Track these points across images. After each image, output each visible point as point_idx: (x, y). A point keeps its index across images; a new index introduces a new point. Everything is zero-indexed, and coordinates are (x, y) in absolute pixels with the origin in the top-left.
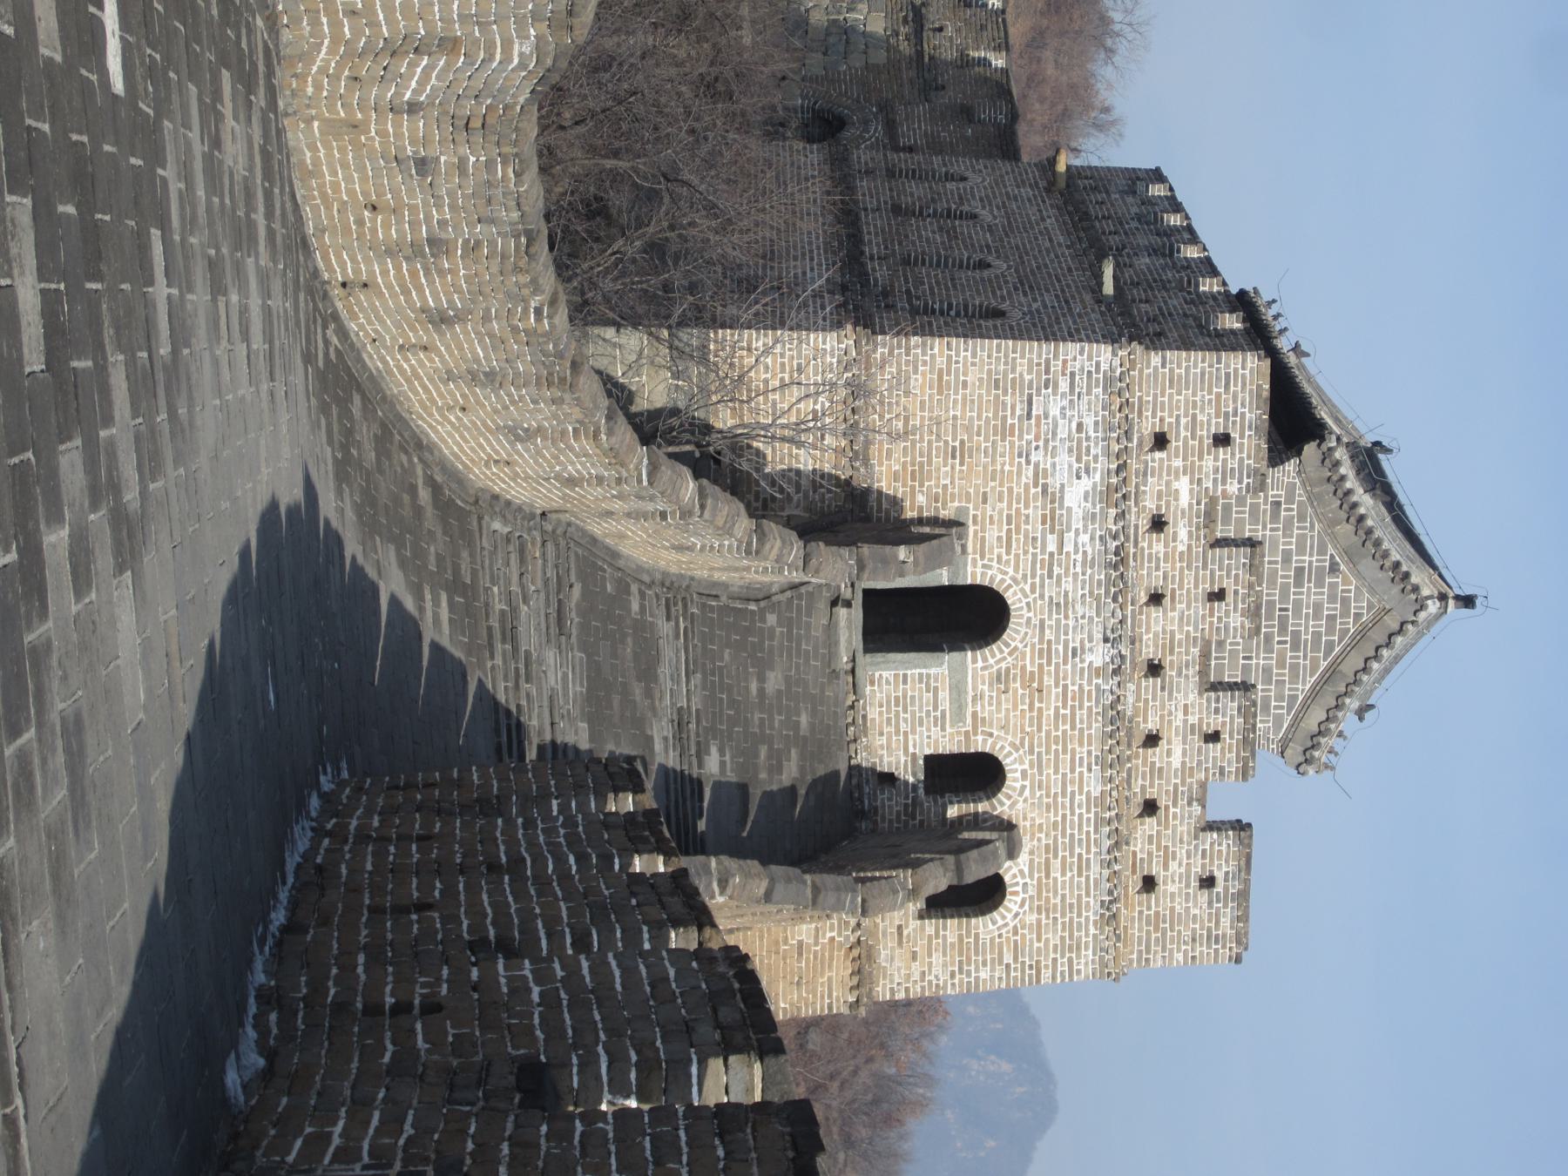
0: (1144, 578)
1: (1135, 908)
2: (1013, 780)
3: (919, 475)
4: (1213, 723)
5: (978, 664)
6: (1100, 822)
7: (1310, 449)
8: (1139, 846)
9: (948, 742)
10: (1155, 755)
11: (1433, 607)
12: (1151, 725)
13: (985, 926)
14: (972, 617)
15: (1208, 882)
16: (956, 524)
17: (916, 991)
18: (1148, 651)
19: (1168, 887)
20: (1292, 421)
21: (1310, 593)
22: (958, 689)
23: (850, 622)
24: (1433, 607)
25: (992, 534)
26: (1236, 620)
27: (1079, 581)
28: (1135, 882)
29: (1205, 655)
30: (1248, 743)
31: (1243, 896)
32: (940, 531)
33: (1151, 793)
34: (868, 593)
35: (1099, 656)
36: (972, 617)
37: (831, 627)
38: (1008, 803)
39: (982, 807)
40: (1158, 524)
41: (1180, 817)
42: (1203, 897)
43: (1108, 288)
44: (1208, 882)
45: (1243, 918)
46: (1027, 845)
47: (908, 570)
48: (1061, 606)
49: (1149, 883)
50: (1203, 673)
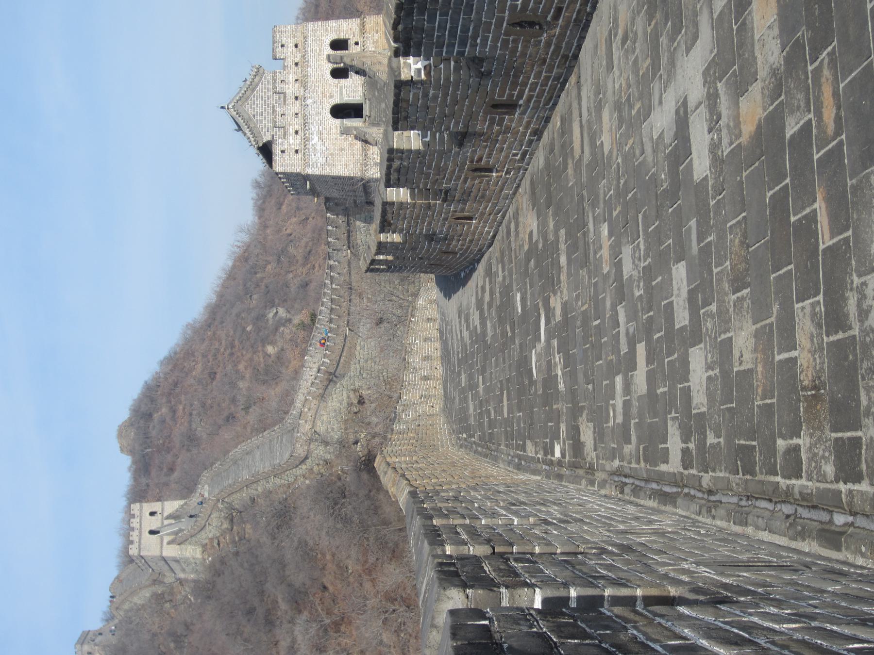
0: (300, 120)
1: (299, 40)
2: (328, 72)
3: (351, 145)
4: (282, 85)
5: (337, 100)
6: (308, 61)
7: (261, 145)
8: (299, 55)
9: (343, 82)
10: (296, 77)
11: (230, 106)
12: (297, 85)
13: (334, 36)
15: (282, 46)
16: (342, 133)
17: (350, 20)
18: (298, 102)
19: (292, 45)
20: (266, 151)
21: (259, 110)
22: (341, 94)
23: (366, 111)
24: (230, 106)
25: (334, 131)
26: (278, 109)
27: (314, 120)
28: (299, 46)
29: (285, 101)
30: (274, 80)
31: (274, 42)
32: (345, 131)
33: (296, 68)
34: (361, 116)
35: (309, 101)
37: (370, 111)
38: (329, 67)
39: (335, 66)
40: (297, 132)
41: (289, 62)
42: (283, 42)
43: (308, 183)
44: (282, 46)
45: (274, 37)
46: (325, 57)
48: (318, 114)
49: (296, 46)
50: (285, 97)
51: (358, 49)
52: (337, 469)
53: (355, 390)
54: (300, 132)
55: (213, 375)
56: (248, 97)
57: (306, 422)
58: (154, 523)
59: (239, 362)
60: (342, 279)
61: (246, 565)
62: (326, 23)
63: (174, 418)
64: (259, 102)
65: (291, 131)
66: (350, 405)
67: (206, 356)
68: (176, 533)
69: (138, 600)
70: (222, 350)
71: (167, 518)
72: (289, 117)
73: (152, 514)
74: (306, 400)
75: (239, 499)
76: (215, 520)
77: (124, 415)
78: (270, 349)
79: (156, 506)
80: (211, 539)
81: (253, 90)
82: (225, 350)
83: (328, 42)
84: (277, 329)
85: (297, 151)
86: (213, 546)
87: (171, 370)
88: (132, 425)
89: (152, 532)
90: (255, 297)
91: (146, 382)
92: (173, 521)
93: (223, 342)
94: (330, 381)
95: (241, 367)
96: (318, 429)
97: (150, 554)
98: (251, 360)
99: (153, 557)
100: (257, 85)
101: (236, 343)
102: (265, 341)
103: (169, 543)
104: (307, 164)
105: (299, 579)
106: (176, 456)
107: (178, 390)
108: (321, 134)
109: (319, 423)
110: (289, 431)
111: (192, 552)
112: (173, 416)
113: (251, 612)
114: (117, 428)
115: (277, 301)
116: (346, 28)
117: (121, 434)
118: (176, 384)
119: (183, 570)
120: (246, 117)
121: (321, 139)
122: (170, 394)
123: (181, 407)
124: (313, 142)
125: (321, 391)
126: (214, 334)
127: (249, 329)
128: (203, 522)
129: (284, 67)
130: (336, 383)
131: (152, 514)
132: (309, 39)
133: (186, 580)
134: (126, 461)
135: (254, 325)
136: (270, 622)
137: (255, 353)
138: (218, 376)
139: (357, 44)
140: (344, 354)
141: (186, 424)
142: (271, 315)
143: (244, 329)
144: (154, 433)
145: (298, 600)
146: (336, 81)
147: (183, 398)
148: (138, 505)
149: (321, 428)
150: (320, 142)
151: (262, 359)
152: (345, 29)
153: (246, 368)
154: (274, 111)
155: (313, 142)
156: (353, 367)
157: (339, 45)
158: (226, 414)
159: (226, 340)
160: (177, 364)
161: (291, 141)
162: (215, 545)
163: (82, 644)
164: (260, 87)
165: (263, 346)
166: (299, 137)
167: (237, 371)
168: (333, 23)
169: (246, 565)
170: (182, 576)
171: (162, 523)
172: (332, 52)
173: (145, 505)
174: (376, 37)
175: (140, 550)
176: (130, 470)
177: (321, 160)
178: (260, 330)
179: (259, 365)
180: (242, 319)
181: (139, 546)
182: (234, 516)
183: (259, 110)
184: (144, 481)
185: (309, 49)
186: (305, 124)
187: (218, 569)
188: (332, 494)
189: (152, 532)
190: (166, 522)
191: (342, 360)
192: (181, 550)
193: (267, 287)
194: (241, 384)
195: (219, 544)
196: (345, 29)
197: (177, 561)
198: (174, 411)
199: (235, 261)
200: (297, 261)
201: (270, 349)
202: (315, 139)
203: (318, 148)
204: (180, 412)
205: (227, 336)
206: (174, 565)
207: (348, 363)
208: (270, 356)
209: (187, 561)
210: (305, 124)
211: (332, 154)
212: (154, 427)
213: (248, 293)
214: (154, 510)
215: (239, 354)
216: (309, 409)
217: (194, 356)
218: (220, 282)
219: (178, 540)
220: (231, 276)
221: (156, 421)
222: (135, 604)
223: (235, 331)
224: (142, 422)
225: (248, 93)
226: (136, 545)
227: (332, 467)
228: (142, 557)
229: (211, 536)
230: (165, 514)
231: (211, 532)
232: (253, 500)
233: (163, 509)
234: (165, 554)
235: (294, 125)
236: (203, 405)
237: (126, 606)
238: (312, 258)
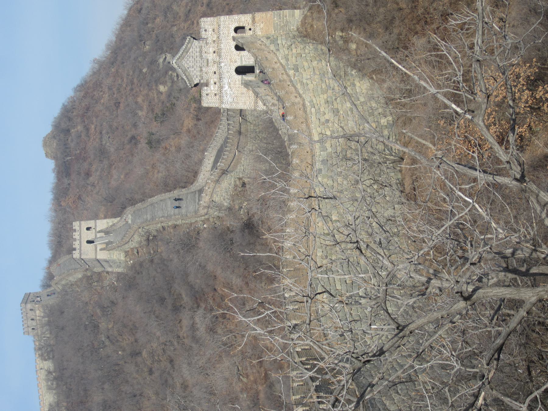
1: (216, 27)
5: (239, 64)
8: (216, 36)
10: (214, 50)
15: (205, 30)
17: (246, 15)
25: (238, 82)
27: (226, 75)
29: (208, 64)
35: (222, 65)
38: (233, 44)
41: (210, 41)
47: (249, 77)
48: (228, 72)
51: (251, 33)
52: (228, 223)
53: (240, 179)
54: (217, 83)
55: (117, 104)
56: (184, 57)
57: (206, 195)
58: (90, 236)
59: (137, 96)
60: (235, 129)
61: (159, 270)
62: (231, 17)
63: (88, 136)
64: (191, 59)
65: (212, 82)
66: (236, 186)
67: (112, 89)
68: (107, 244)
69: (72, 279)
70: (124, 86)
71: (100, 232)
72: (211, 74)
73: (88, 229)
74: (207, 183)
75: (153, 228)
76: (137, 238)
77: (48, 129)
78: (162, 88)
79: (91, 223)
80: (132, 249)
81: (187, 52)
82: (126, 86)
83: (233, 28)
84: (166, 73)
85: (215, 95)
86: (134, 254)
87: (84, 97)
88: (54, 137)
89: (89, 242)
90: (148, 43)
91: (63, 105)
92: (102, 234)
93: (125, 80)
94: (223, 173)
95: (140, 100)
96: (214, 199)
97: (88, 257)
98: (147, 95)
99: (91, 260)
100: (189, 49)
101: (135, 81)
102: (158, 82)
103: (101, 250)
104: (222, 102)
105: (197, 281)
106: (91, 164)
107: (90, 114)
108: (230, 84)
109: (215, 196)
110: (192, 192)
111: (118, 256)
112: (87, 133)
113: (162, 300)
114: (43, 139)
115: (165, 49)
116: (244, 20)
117: (46, 143)
118: (88, 109)
119: (111, 266)
120: (184, 69)
121: (230, 87)
122: (83, 116)
123: (93, 127)
124: (225, 89)
125: (217, 178)
126: (117, 71)
127: (144, 70)
128: (128, 240)
129: (207, 43)
130: (227, 174)
131: (88, 229)
132: (222, 26)
133: (112, 272)
134: (50, 164)
135: (148, 67)
136: (177, 309)
137: (150, 90)
138: (121, 105)
139: (250, 29)
140: (234, 161)
141: (97, 140)
142: (161, 60)
143: (141, 71)
144: (72, 145)
145: (198, 297)
146: (238, 52)
147: (94, 119)
148: (78, 222)
149: (216, 198)
150: (229, 89)
151: (155, 95)
152: (243, 20)
153: (143, 101)
154: (201, 70)
155: (225, 89)
156: (239, 168)
158: (130, 136)
159: (127, 79)
160: (88, 90)
161: (212, 88)
162: (135, 252)
163: (26, 303)
164: (191, 50)
165: (157, 85)
166: (216, 86)
167: (136, 103)
168: (236, 17)
169: (159, 270)
170: (110, 269)
171: (96, 235)
172: (235, 35)
173: (83, 222)
174: (262, 26)
175: (81, 255)
176: (54, 172)
177: (230, 100)
178: (153, 73)
179: (154, 99)
180: (140, 62)
181: (80, 252)
182: (150, 239)
183: (191, 64)
184: (66, 181)
185: (221, 33)
186: (220, 79)
187: (138, 269)
188: (223, 238)
189: (89, 242)
190: (99, 235)
191: (232, 164)
192: (110, 254)
193: (157, 37)
194: (140, 113)
195: (138, 253)
196: (243, 20)
197: (106, 261)
198: (88, 130)
199: (130, 10)
200: (180, 18)
201: (162, 88)
202: (226, 87)
203: (228, 92)
204: (92, 130)
205: (128, 75)
206: (104, 263)
207: (236, 166)
208: (162, 93)
209: (114, 262)
210: (220, 79)
211: (236, 96)
212: (72, 141)
213: (141, 39)
214: (89, 226)
215: (138, 90)
216: (209, 188)
217: (102, 87)
218: (118, 27)
219: (108, 247)
220: (126, 23)
221: (73, 135)
222: (70, 281)
223: (134, 72)
224: (62, 135)
225: (184, 54)
226: (78, 251)
227: (223, 221)
228: (82, 259)
229: (132, 247)
230: (98, 229)
231: (133, 244)
232: (164, 228)
233: (96, 226)
234: (98, 257)
236: (111, 127)
237: (63, 282)
238: (191, 16)
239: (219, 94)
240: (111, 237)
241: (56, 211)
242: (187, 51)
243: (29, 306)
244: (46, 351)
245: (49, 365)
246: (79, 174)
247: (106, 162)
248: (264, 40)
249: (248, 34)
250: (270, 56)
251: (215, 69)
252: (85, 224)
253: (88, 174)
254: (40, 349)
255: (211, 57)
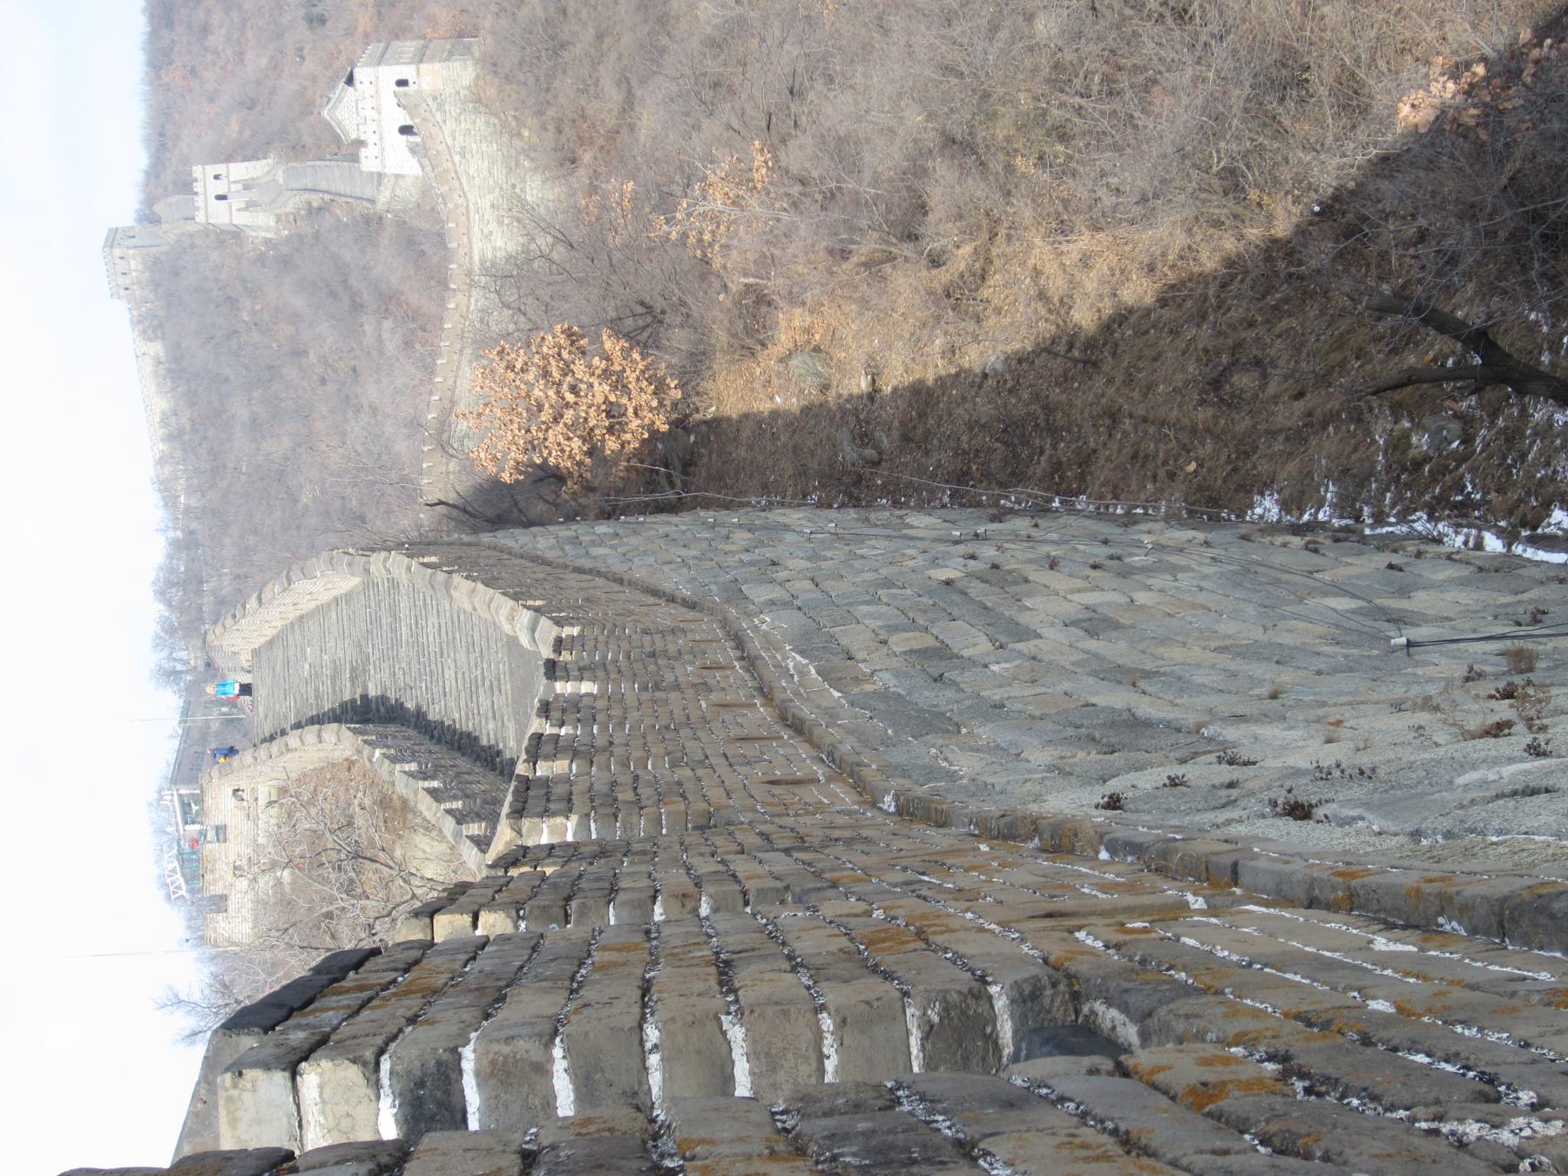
14: (406, 130)
36: (406, 130)
73: (217, 177)
79: (220, 168)
106: (209, 12)
131: (217, 177)
157: (402, 83)
163: (112, 247)
190: (234, 188)
235: (371, 139)
239: (381, 157)
240: (253, 195)
241: (151, 83)
242: (340, 100)
243: (117, 252)
244: (151, 326)
245: (157, 348)
246: (189, 27)
247: (235, 15)
248: (430, 101)
249: (412, 88)
250: (435, 131)
251: (374, 127)
252: (212, 170)
253: (205, 30)
254: (140, 322)
255: (370, 114)
